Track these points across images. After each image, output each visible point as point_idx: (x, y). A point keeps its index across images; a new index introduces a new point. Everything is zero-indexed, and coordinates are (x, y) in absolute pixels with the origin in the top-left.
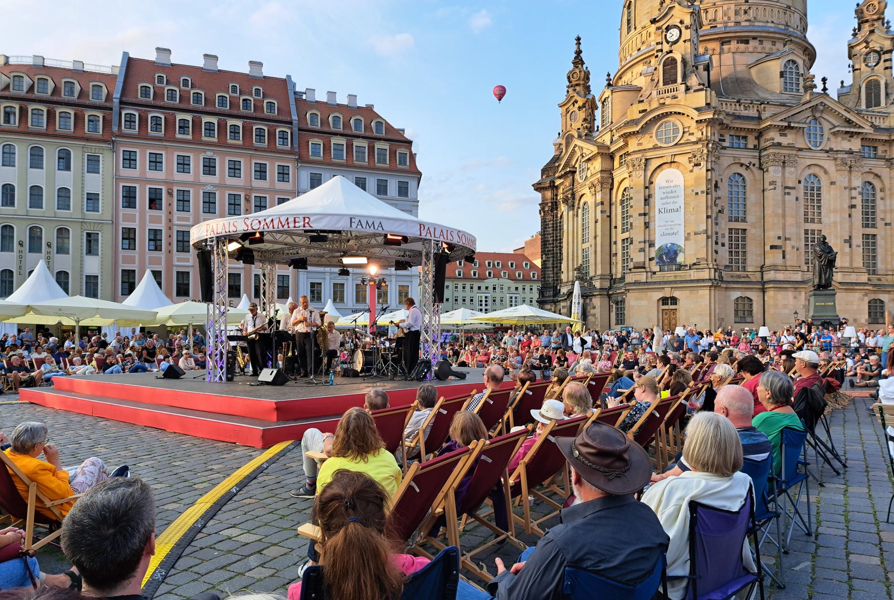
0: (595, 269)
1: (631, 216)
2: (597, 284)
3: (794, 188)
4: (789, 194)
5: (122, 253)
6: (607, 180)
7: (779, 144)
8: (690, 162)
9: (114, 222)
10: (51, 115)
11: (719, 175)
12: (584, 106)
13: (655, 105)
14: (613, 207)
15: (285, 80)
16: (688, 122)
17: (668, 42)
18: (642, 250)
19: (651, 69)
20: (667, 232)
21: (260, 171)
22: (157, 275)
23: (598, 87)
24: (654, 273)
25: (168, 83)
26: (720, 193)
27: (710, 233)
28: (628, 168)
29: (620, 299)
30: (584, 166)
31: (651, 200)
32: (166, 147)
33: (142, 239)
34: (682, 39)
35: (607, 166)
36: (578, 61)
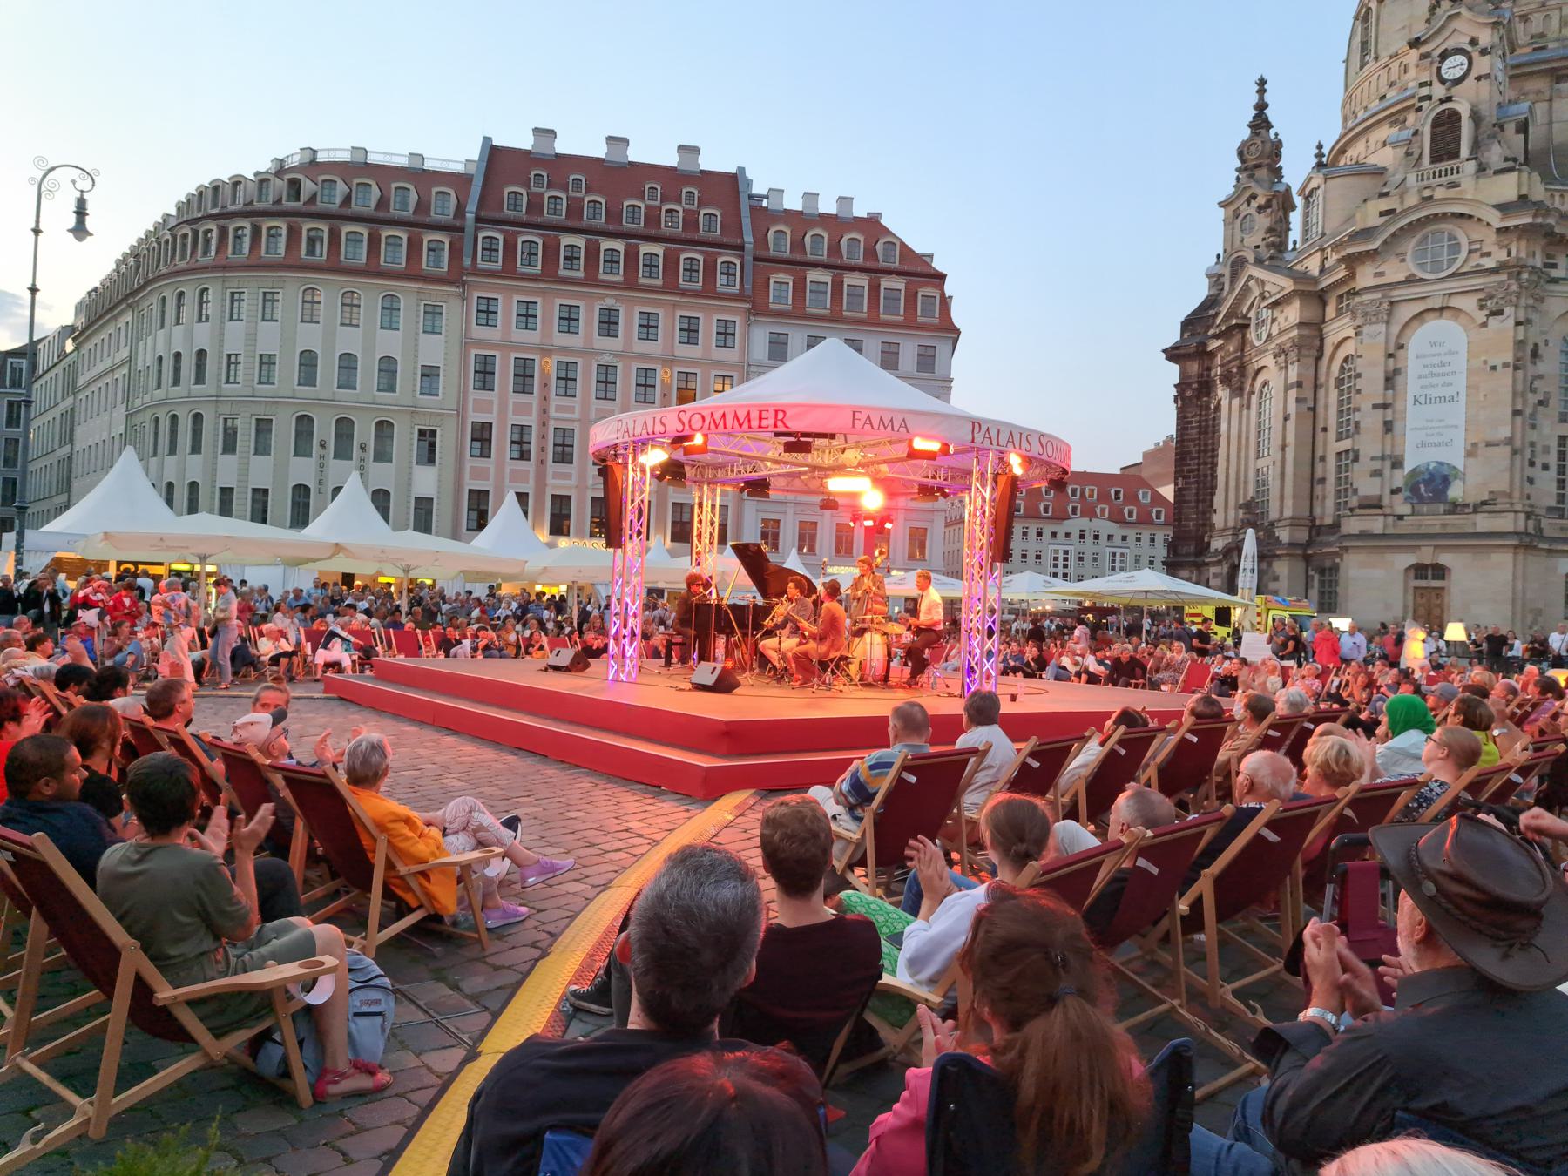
0: (1282, 506)
1: (1357, 409)
2: (1284, 535)
5: (470, 463)
6: (1311, 341)
8: (1482, 307)
9: (461, 413)
10: (374, 241)
11: (1543, 333)
12: (1268, 205)
13: (1412, 200)
14: (1321, 393)
16: (1477, 233)
17: (1443, 81)
18: (1377, 473)
19: (1407, 134)
20: (1431, 440)
21: (689, 330)
22: (522, 497)
23: (1296, 169)
24: (1401, 517)
25: (550, 186)
26: (1541, 367)
27: (1518, 444)
28: (1354, 318)
29: (1328, 564)
30: (1266, 314)
31: (1399, 379)
32: (543, 292)
33: (501, 441)
34: (1474, 74)
35: (1312, 314)
36: (1260, 122)
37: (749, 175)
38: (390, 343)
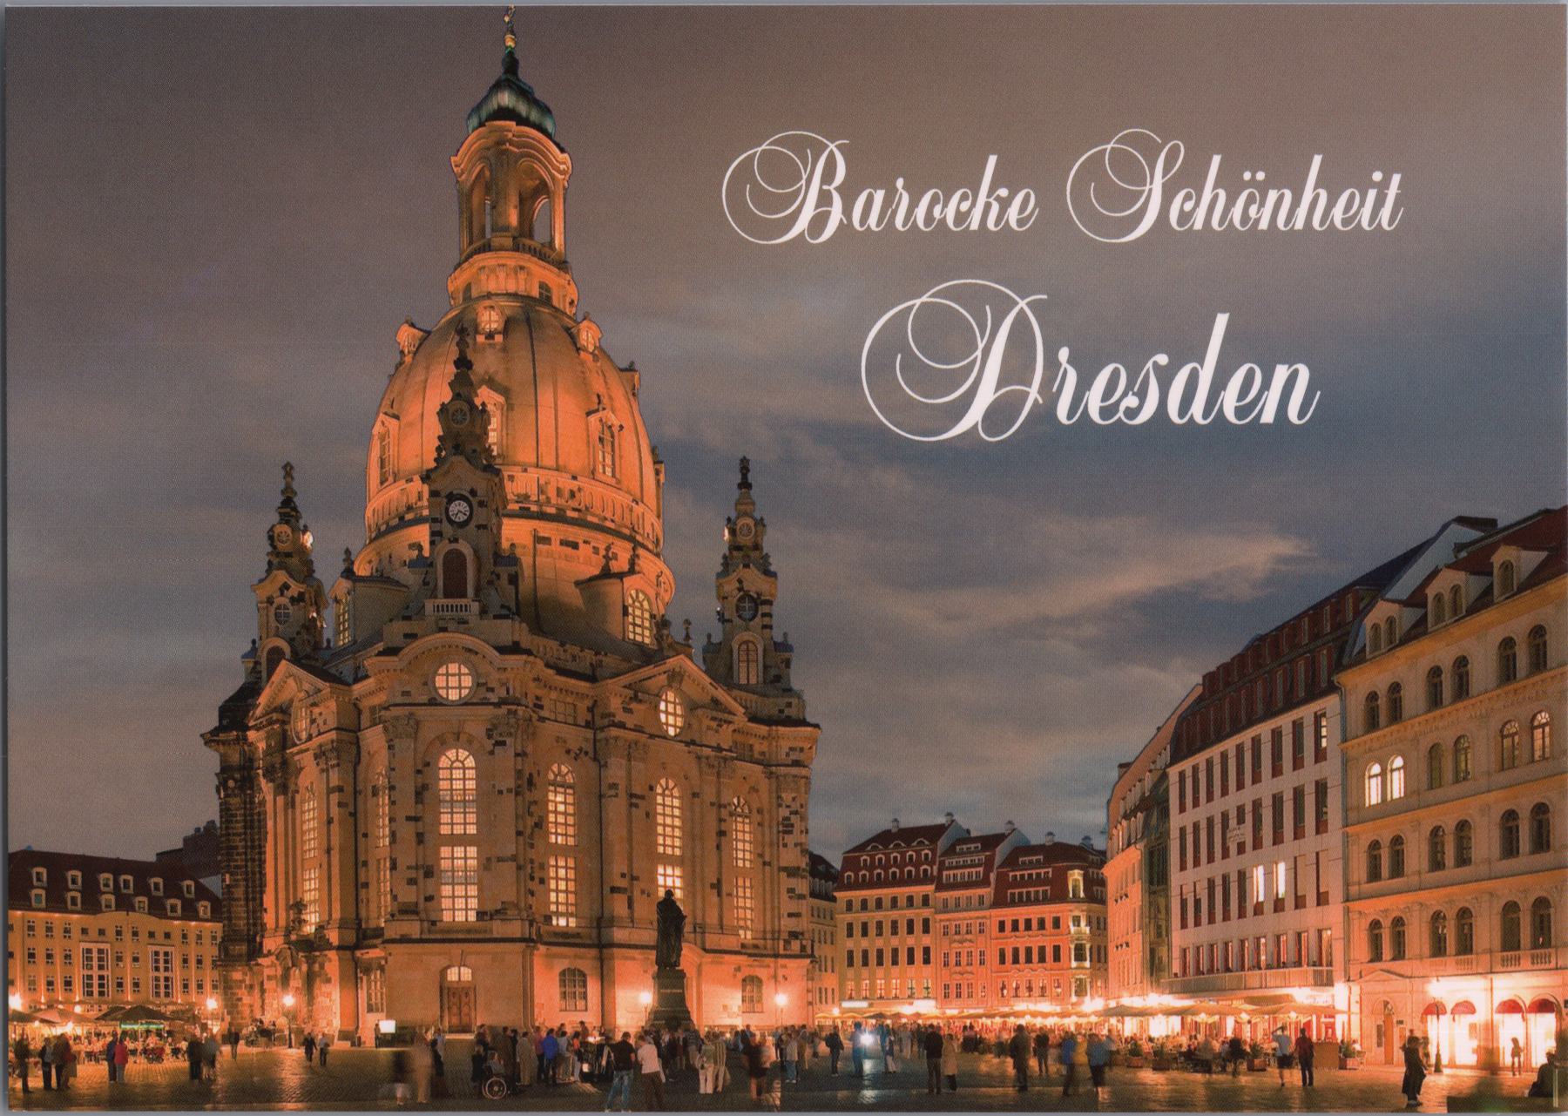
3: (642, 797)
4: (636, 806)
6: (346, 747)
7: (622, 726)
8: (490, 737)
18: (412, 882)
31: (427, 794)
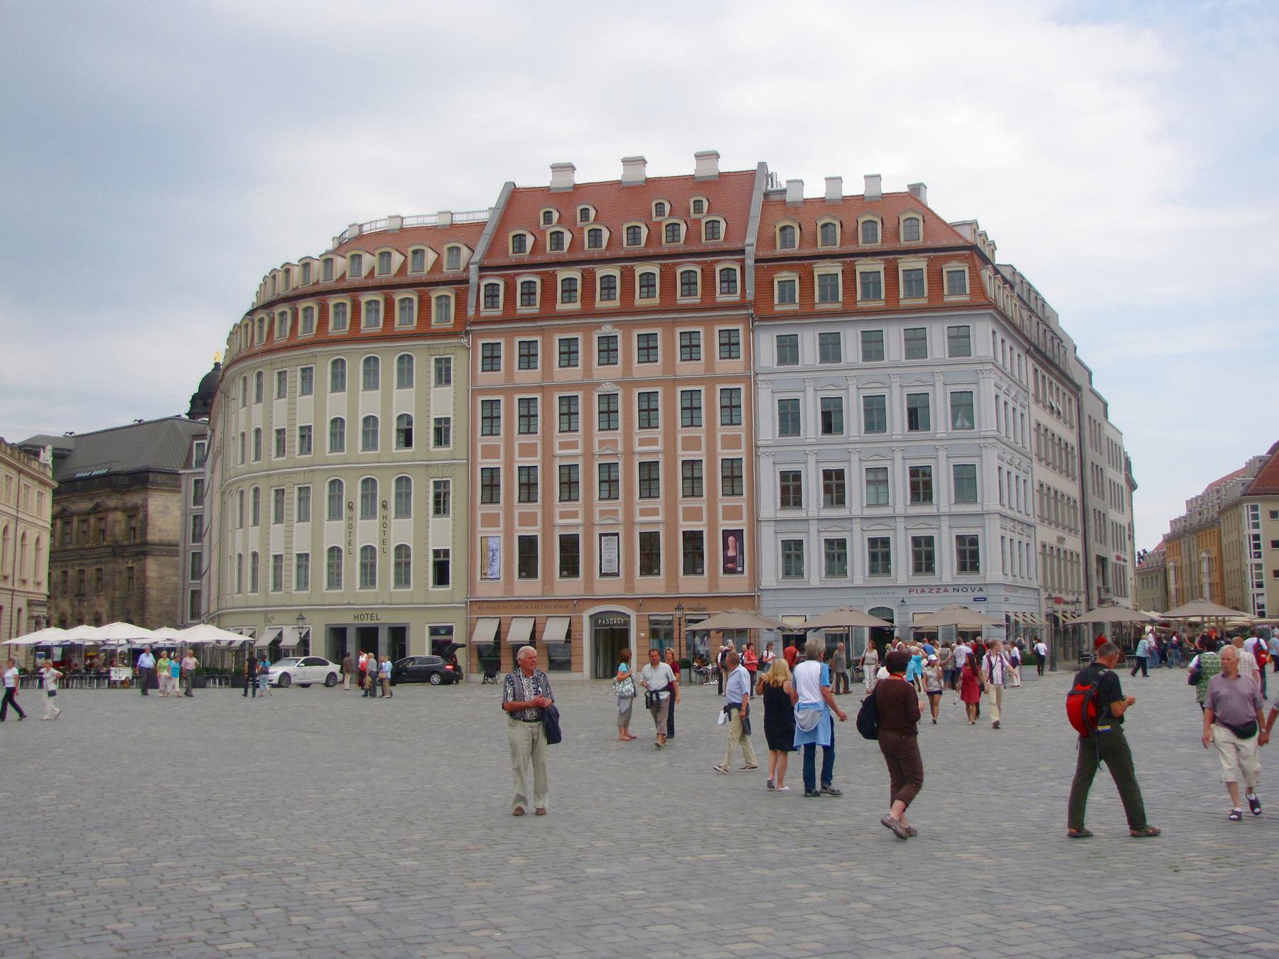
15: (752, 174)
32: (541, 330)
33: (509, 485)
37: (771, 170)
38: (404, 401)
